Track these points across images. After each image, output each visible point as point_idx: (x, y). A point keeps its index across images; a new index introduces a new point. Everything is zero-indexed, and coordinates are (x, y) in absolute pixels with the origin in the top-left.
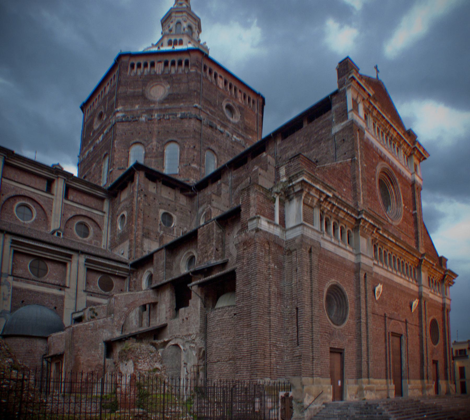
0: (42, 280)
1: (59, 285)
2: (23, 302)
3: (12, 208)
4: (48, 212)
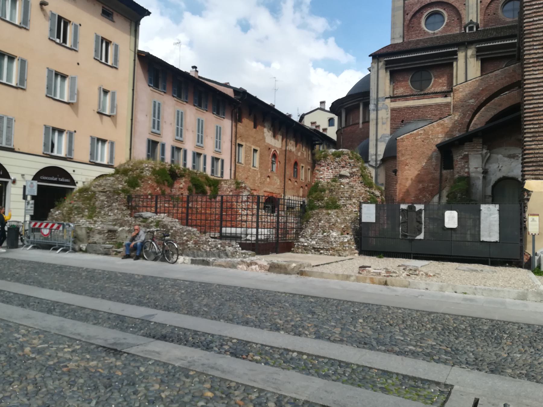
0: (426, 92)
1: (443, 92)
2: (402, 121)
3: (420, 23)
4: (461, 8)
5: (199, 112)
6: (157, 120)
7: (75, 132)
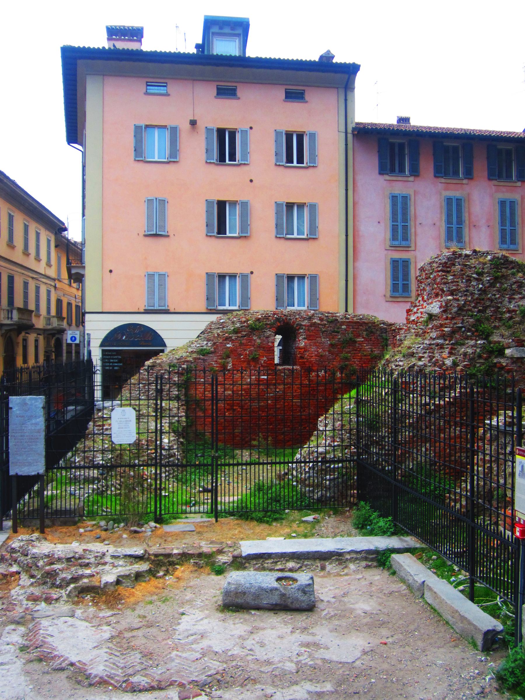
5: (504, 189)
6: (400, 224)
7: (252, 273)
